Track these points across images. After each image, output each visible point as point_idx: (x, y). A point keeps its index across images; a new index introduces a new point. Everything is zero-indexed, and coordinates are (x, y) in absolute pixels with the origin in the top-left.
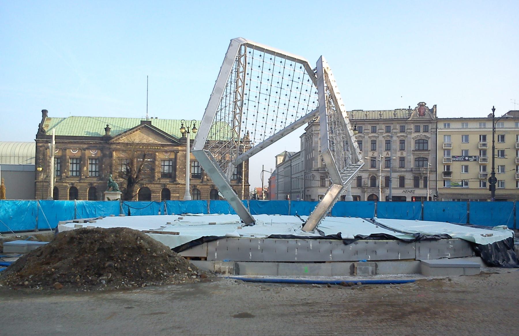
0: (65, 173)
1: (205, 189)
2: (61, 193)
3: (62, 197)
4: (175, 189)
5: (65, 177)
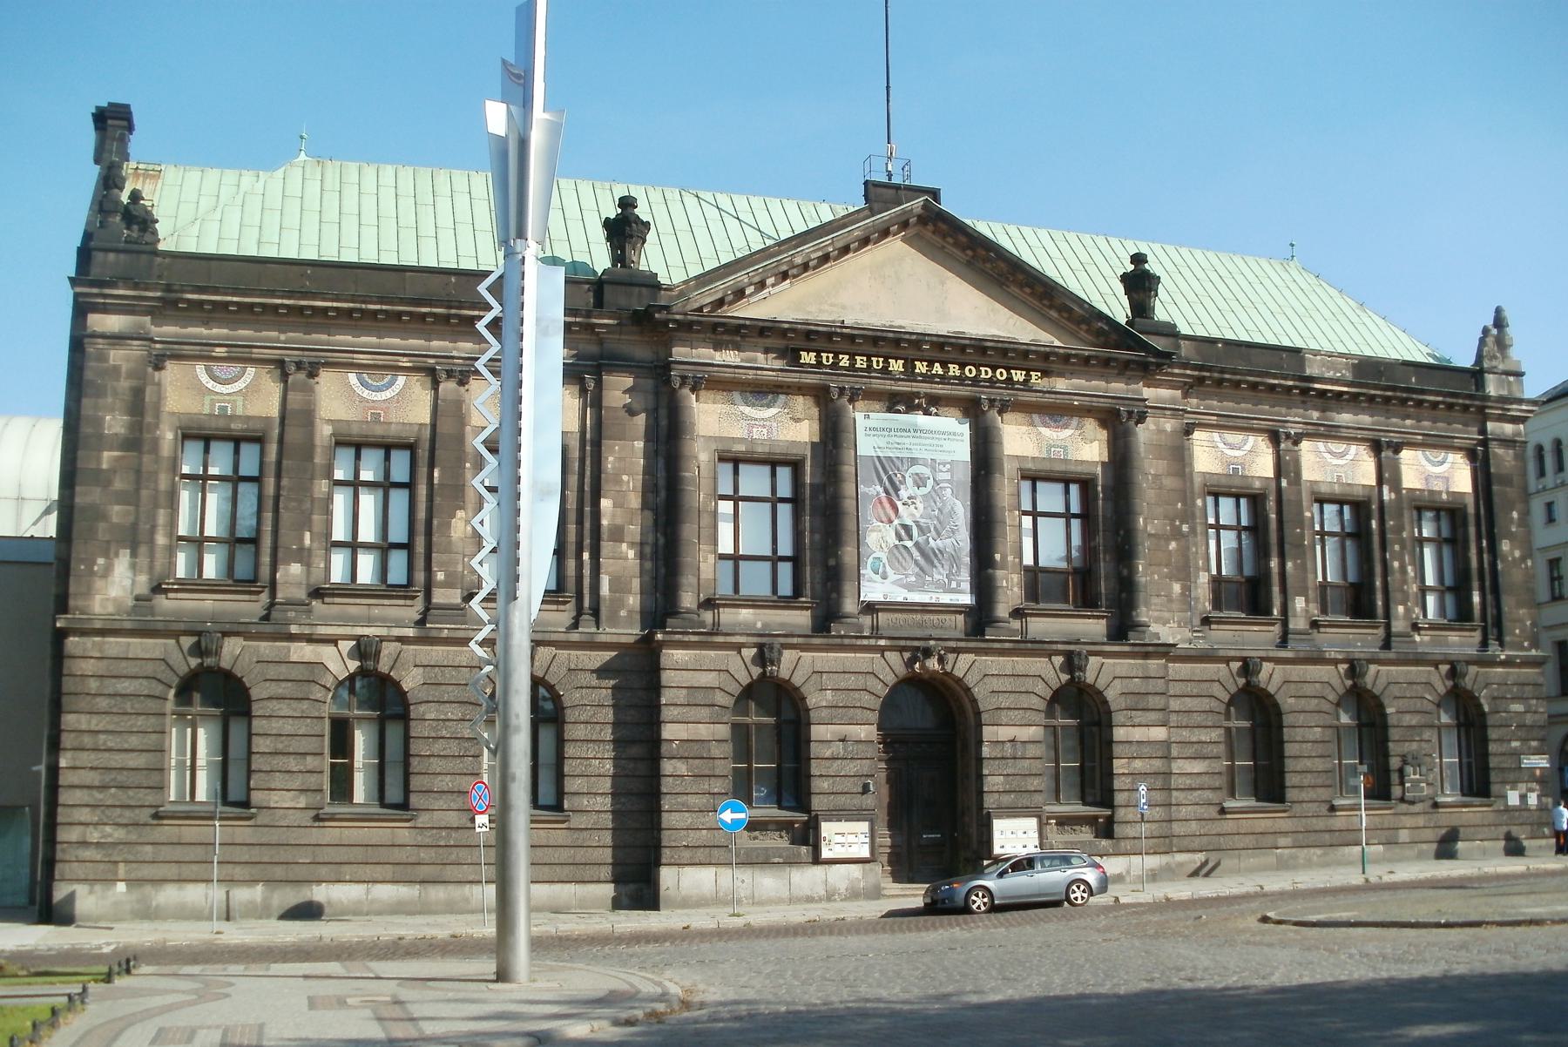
0: (303, 556)
1: (1308, 690)
2: (275, 726)
3: (279, 762)
4: (1136, 685)
5: (301, 594)
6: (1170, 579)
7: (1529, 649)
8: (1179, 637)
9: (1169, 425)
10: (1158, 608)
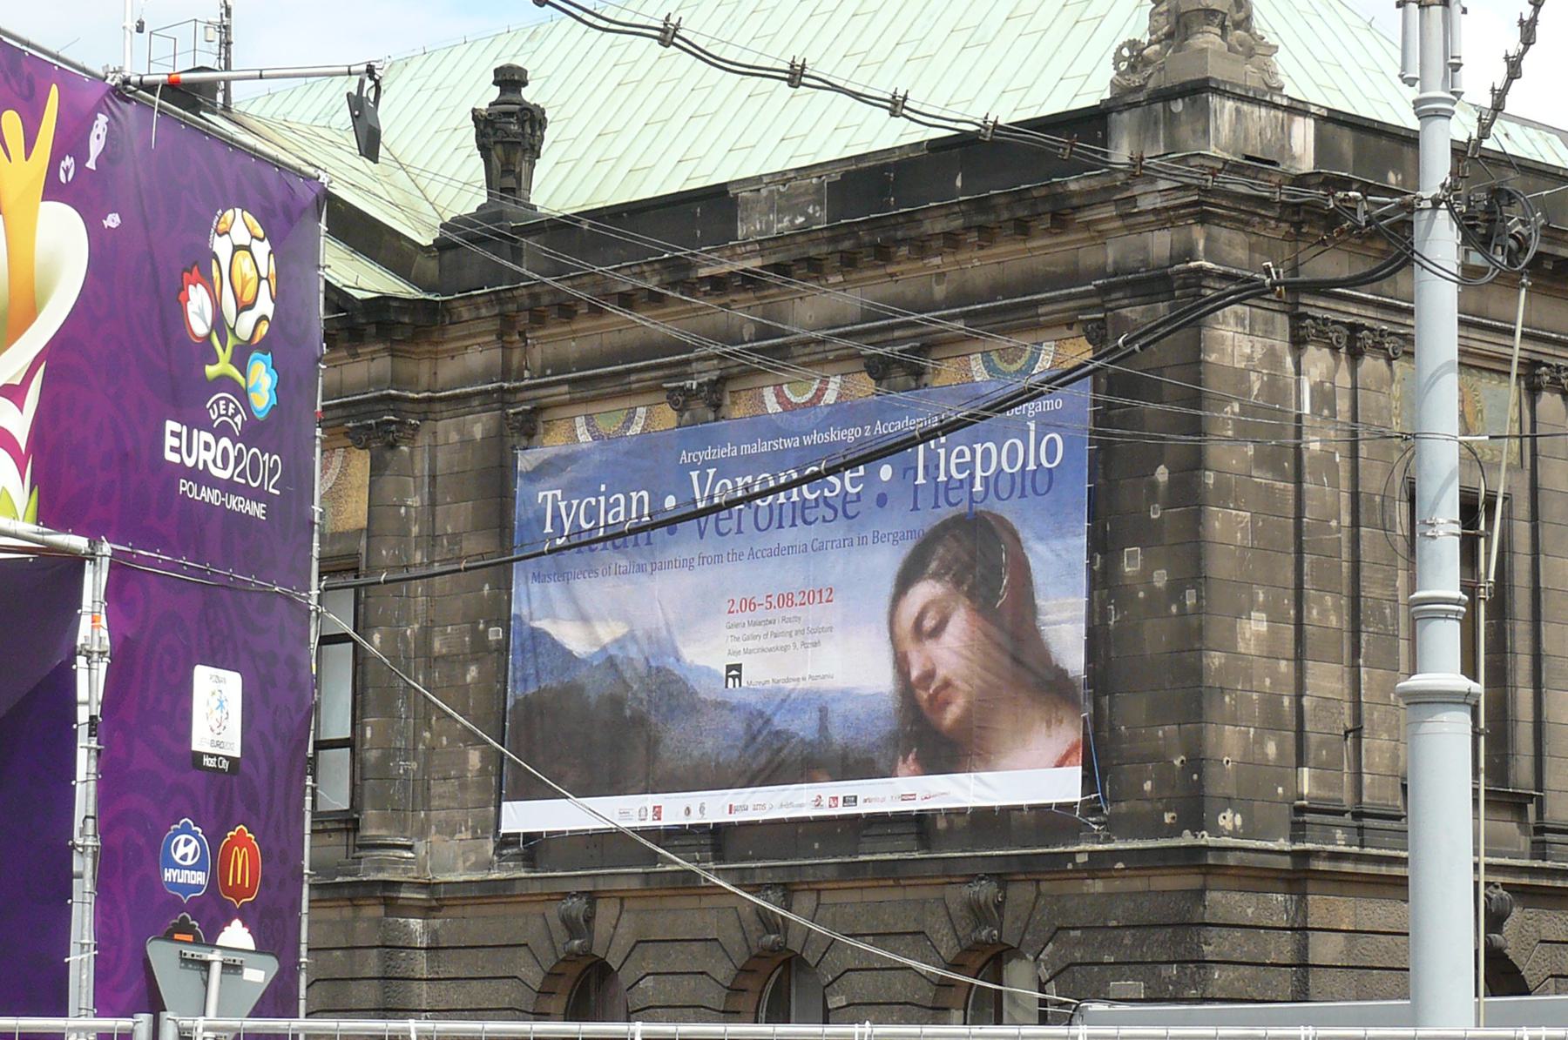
6: (465, 742)
7: (1175, 831)
8: (473, 858)
9: (479, 426)
10: (445, 803)
